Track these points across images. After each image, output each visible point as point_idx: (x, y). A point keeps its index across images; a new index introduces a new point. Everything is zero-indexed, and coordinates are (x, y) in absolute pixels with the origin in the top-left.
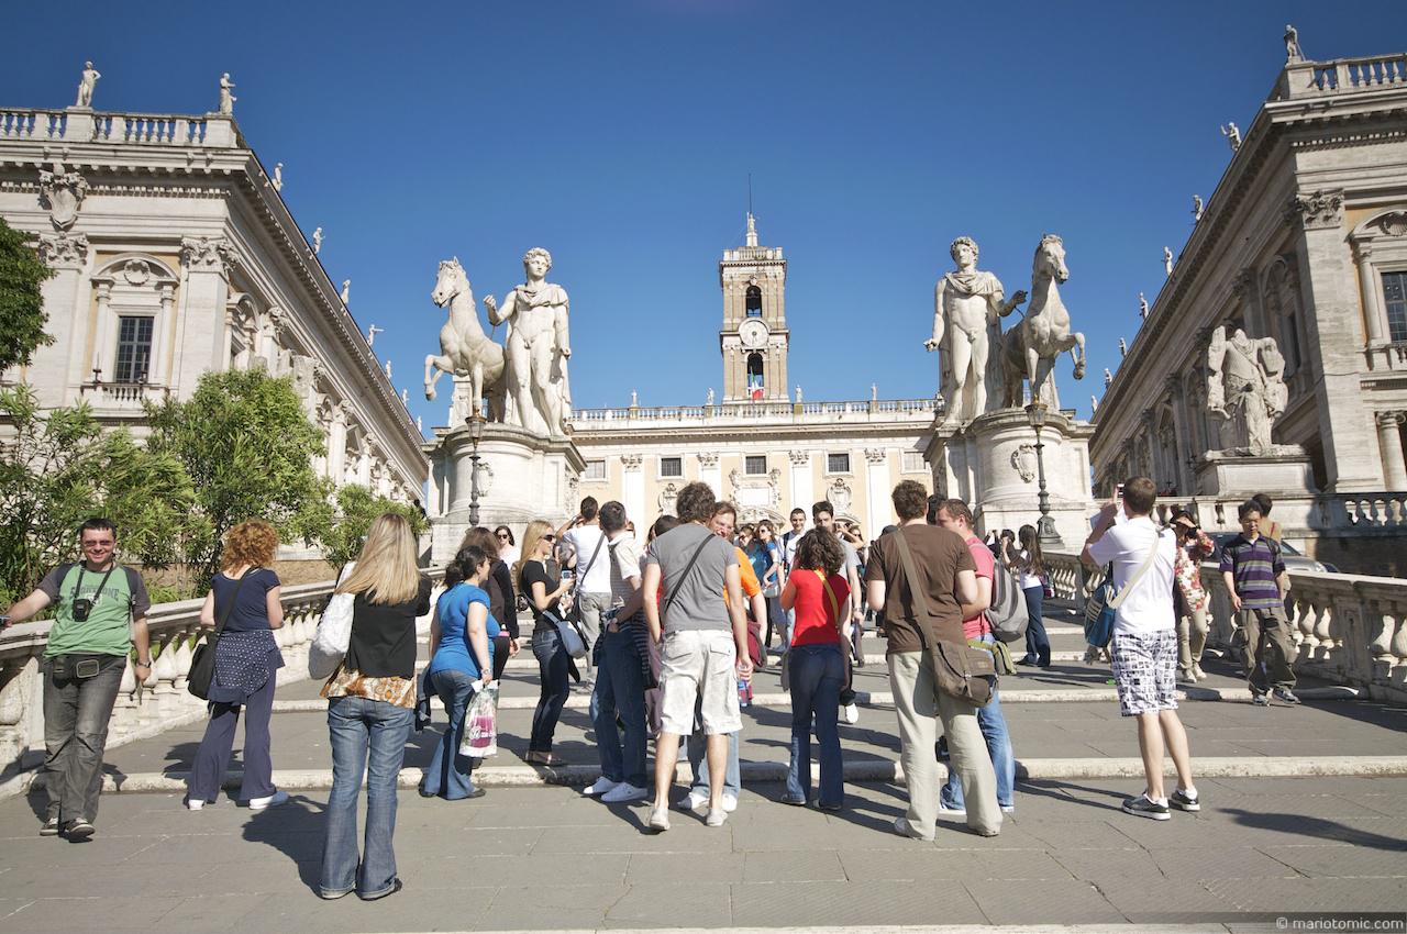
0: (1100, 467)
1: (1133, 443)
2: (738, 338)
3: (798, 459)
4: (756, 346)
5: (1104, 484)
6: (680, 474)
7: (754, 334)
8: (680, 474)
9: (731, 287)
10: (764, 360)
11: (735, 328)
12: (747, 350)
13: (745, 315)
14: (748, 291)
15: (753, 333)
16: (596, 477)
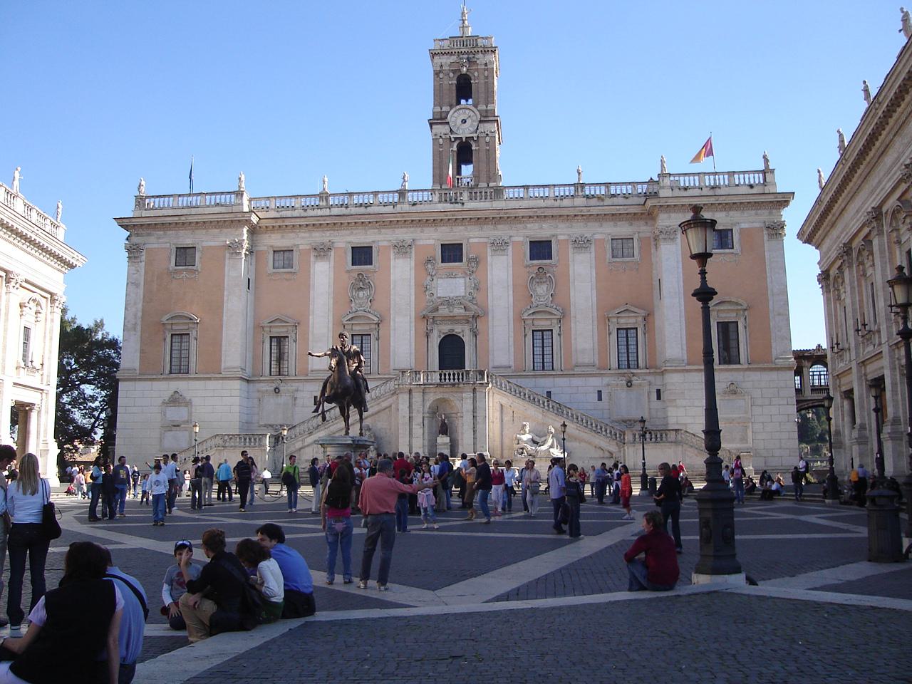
0: (829, 250)
1: (881, 213)
2: (447, 127)
3: (500, 246)
4: (465, 131)
5: (833, 272)
6: (371, 264)
7: (464, 121)
8: (371, 264)
9: (441, 75)
10: (473, 148)
11: (443, 115)
12: (456, 139)
13: (454, 101)
14: (459, 79)
15: (463, 121)
16: (284, 268)
